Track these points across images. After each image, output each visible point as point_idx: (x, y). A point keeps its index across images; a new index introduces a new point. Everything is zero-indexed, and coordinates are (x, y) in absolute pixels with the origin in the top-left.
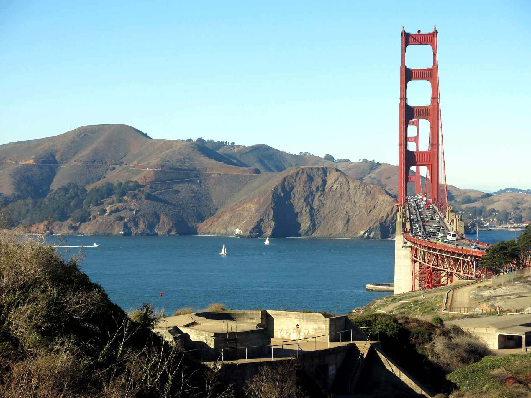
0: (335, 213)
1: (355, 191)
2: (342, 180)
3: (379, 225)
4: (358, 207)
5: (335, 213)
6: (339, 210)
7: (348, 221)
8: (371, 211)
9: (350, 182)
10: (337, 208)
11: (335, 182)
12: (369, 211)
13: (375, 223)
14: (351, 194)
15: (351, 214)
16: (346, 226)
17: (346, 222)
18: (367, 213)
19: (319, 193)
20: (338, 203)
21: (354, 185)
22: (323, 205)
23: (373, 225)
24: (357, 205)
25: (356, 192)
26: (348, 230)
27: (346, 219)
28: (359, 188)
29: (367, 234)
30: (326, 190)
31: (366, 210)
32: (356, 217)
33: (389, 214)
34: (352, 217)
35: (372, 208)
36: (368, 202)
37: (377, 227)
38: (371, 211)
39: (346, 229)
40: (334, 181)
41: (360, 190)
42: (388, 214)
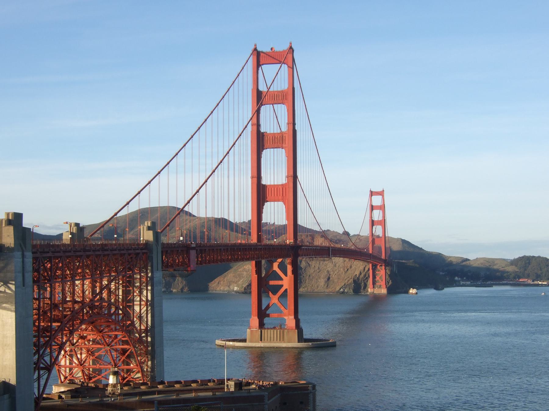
3: (353, 282)
4: (337, 267)
5: (319, 272)
7: (329, 279)
8: (348, 270)
10: (320, 268)
13: (349, 280)
15: (332, 273)
16: (327, 283)
17: (326, 280)
18: (345, 271)
23: (348, 282)
24: (337, 265)
26: (328, 287)
27: (327, 277)
29: (342, 290)
31: (344, 269)
33: (362, 273)
35: (349, 267)
36: (345, 263)
37: (350, 283)
38: (348, 270)
39: (327, 285)
42: (360, 272)
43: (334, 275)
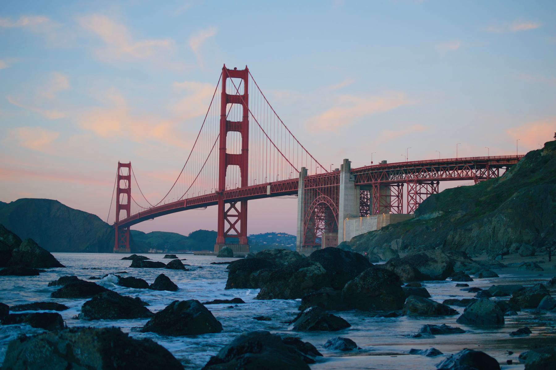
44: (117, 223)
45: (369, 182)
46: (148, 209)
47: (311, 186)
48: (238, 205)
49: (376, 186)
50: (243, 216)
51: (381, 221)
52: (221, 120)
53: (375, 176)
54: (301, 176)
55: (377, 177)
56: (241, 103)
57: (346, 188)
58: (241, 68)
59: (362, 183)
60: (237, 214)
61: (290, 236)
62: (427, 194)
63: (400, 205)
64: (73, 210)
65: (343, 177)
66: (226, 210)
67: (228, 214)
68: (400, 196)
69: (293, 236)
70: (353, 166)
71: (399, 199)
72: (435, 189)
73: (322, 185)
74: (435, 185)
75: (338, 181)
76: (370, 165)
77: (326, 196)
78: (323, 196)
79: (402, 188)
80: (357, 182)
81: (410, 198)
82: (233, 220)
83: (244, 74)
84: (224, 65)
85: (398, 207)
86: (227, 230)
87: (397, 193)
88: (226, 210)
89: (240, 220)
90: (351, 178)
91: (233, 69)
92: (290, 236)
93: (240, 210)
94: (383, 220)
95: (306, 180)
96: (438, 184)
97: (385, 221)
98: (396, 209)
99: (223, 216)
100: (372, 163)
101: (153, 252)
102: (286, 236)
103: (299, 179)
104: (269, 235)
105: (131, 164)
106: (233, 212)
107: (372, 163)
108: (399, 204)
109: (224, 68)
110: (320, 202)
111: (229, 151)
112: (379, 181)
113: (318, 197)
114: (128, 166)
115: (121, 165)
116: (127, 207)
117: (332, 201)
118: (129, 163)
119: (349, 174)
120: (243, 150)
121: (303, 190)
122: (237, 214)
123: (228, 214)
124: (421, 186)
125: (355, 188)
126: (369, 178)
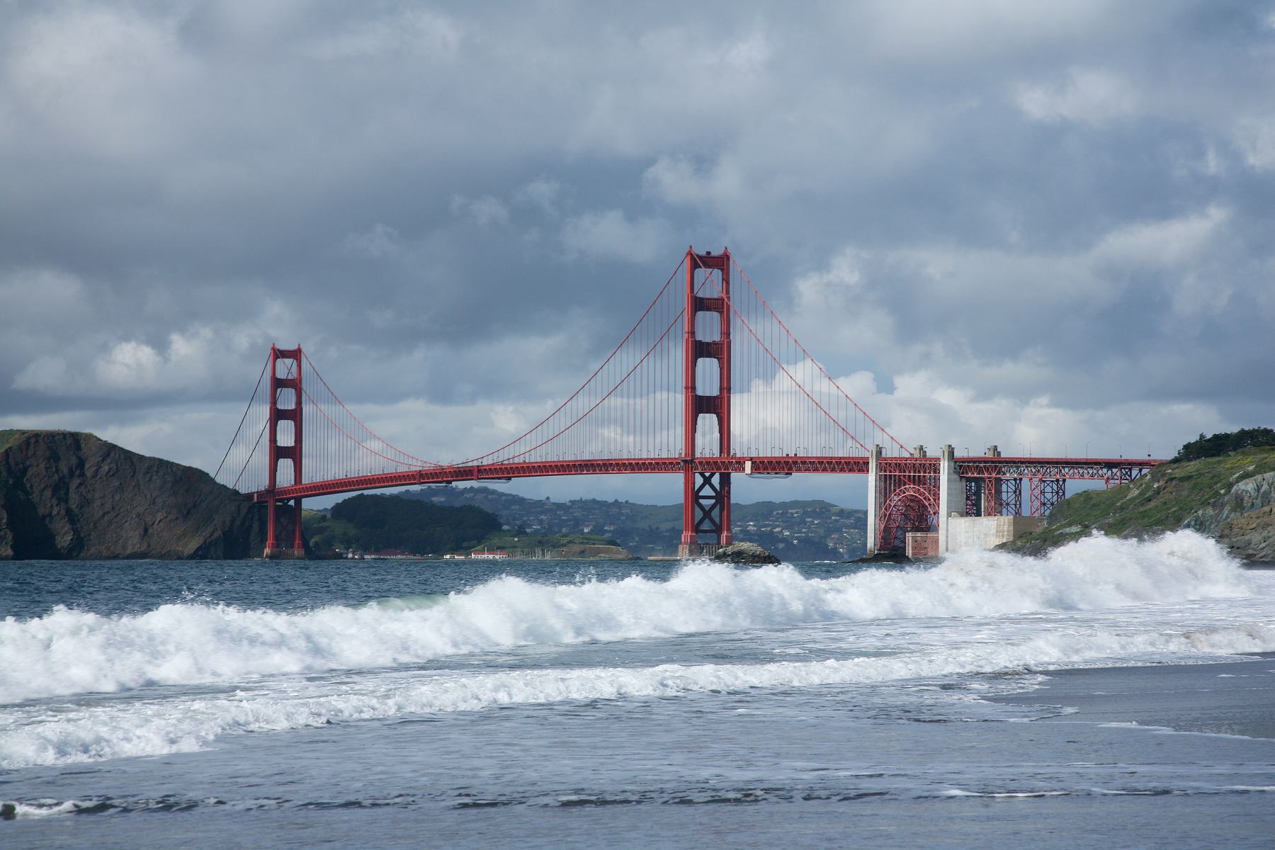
0: (116, 516)
1: (149, 476)
2: (117, 456)
6: (122, 510)
9: (135, 460)
11: (103, 460)
12: (185, 512)
14: (141, 483)
15: (149, 519)
19: (76, 482)
20: (117, 498)
21: (146, 465)
22: (88, 503)
25: (150, 479)
28: (157, 472)
30: (89, 474)
32: (160, 524)
34: (154, 523)
40: (101, 459)
41: (160, 474)
43: (156, 523)
44: (272, 490)
45: (978, 476)
46: (425, 469)
47: (891, 472)
48: (716, 480)
49: (990, 481)
50: (722, 496)
51: (1002, 523)
52: (687, 340)
53: (988, 470)
54: (874, 456)
55: (992, 470)
56: (716, 309)
57: (949, 480)
58: (717, 252)
59: (970, 475)
60: (714, 494)
61: (503, 498)
62: (1052, 492)
63: (1018, 503)
64: (141, 457)
65: (944, 467)
66: (696, 489)
67: (701, 494)
68: (1018, 492)
69: (514, 496)
70: (958, 454)
71: (1016, 495)
72: (1061, 486)
73: (910, 472)
74: (1061, 483)
75: (937, 470)
76: (983, 455)
77: (917, 487)
78: (912, 486)
79: (1020, 482)
80: (963, 473)
81: (1033, 498)
82: (707, 503)
83: (720, 262)
84: (691, 247)
85: (1015, 505)
86: (700, 520)
87: (1014, 488)
88: (696, 489)
89: (718, 506)
90: (955, 468)
91: (703, 253)
92: (503, 498)
93: (718, 487)
94: (1004, 522)
95: (880, 463)
96: (1064, 481)
97: (1007, 523)
98: (1013, 507)
99: (694, 496)
100: (985, 454)
101: (356, 557)
102: (490, 497)
103: (870, 461)
104: (434, 496)
105: (303, 350)
106: (707, 491)
107: (985, 454)
108: (1016, 502)
109: (690, 254)
110: (907, 493)
111: (700, 392)
112: (994, 475)
113: (903, 488)
114: (296, 354)
115: (278, 354)
116: (294, 453)
117: (927, 494)
118: (294, 347)
119: (953, 464)
120: (721, 389)
121: (878, 475)
122: (714, 494)
123: (701, 494)
124: (1046, 485)
125: (961, 480)
126: (979, 470)
